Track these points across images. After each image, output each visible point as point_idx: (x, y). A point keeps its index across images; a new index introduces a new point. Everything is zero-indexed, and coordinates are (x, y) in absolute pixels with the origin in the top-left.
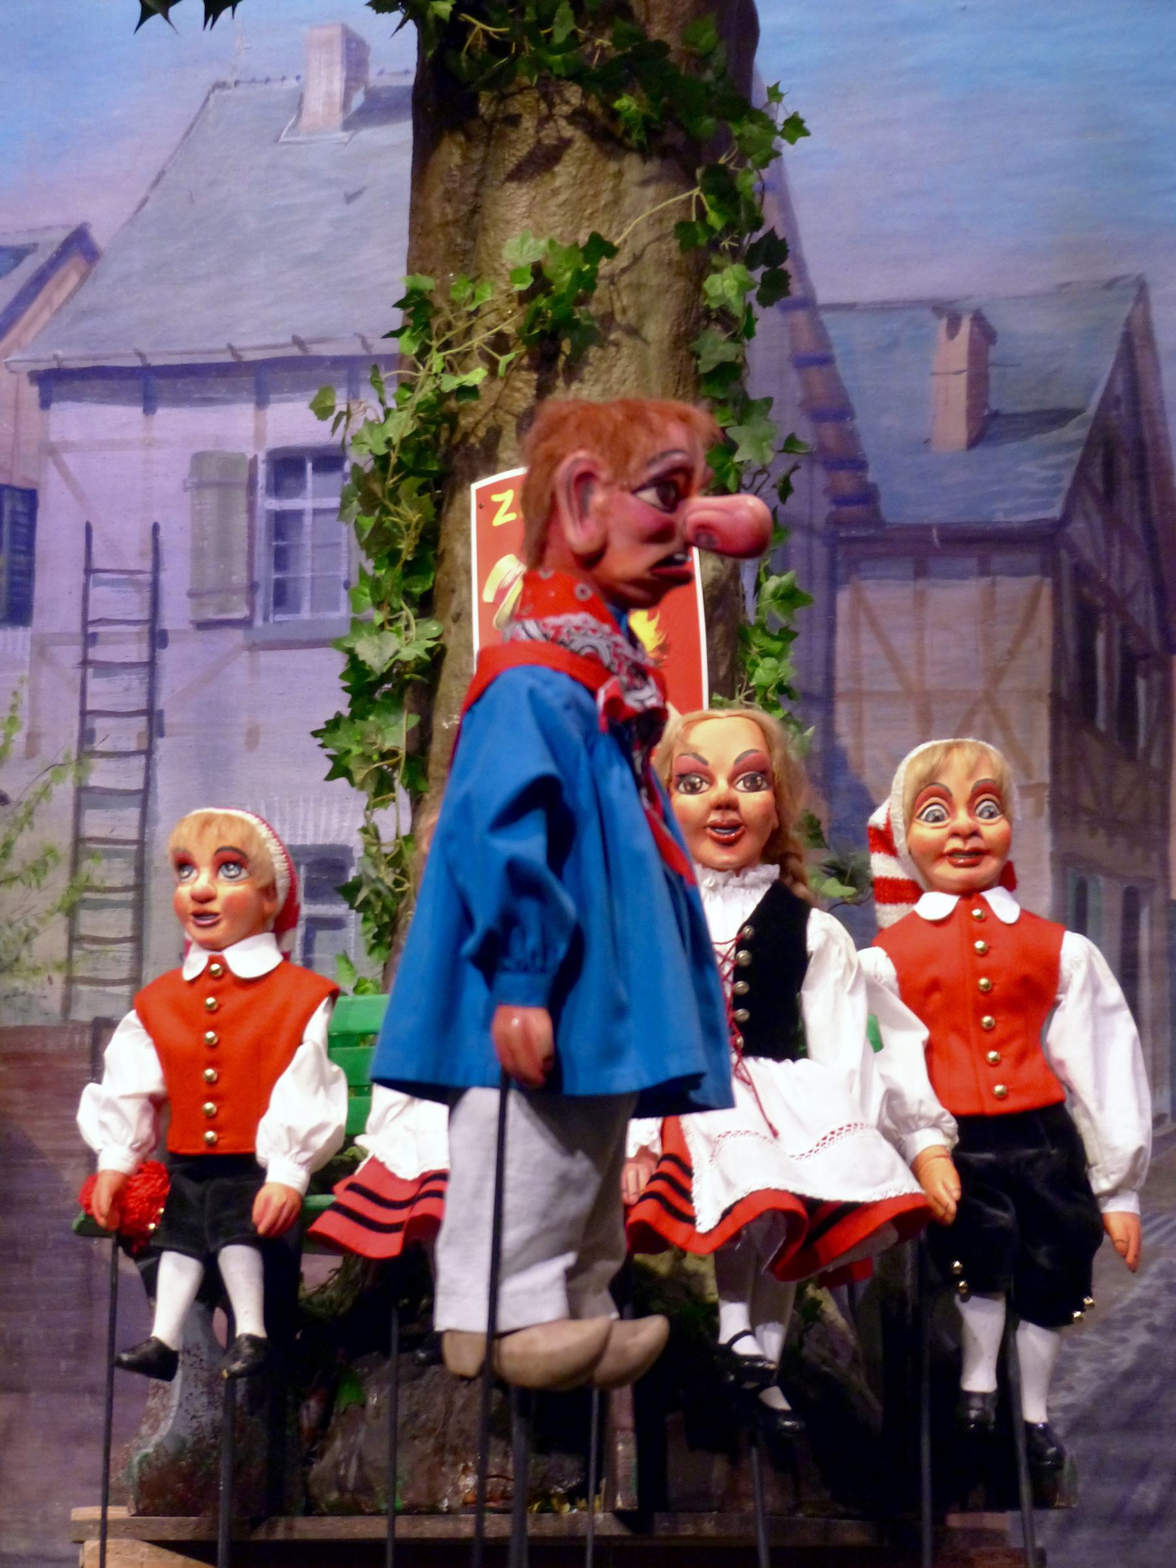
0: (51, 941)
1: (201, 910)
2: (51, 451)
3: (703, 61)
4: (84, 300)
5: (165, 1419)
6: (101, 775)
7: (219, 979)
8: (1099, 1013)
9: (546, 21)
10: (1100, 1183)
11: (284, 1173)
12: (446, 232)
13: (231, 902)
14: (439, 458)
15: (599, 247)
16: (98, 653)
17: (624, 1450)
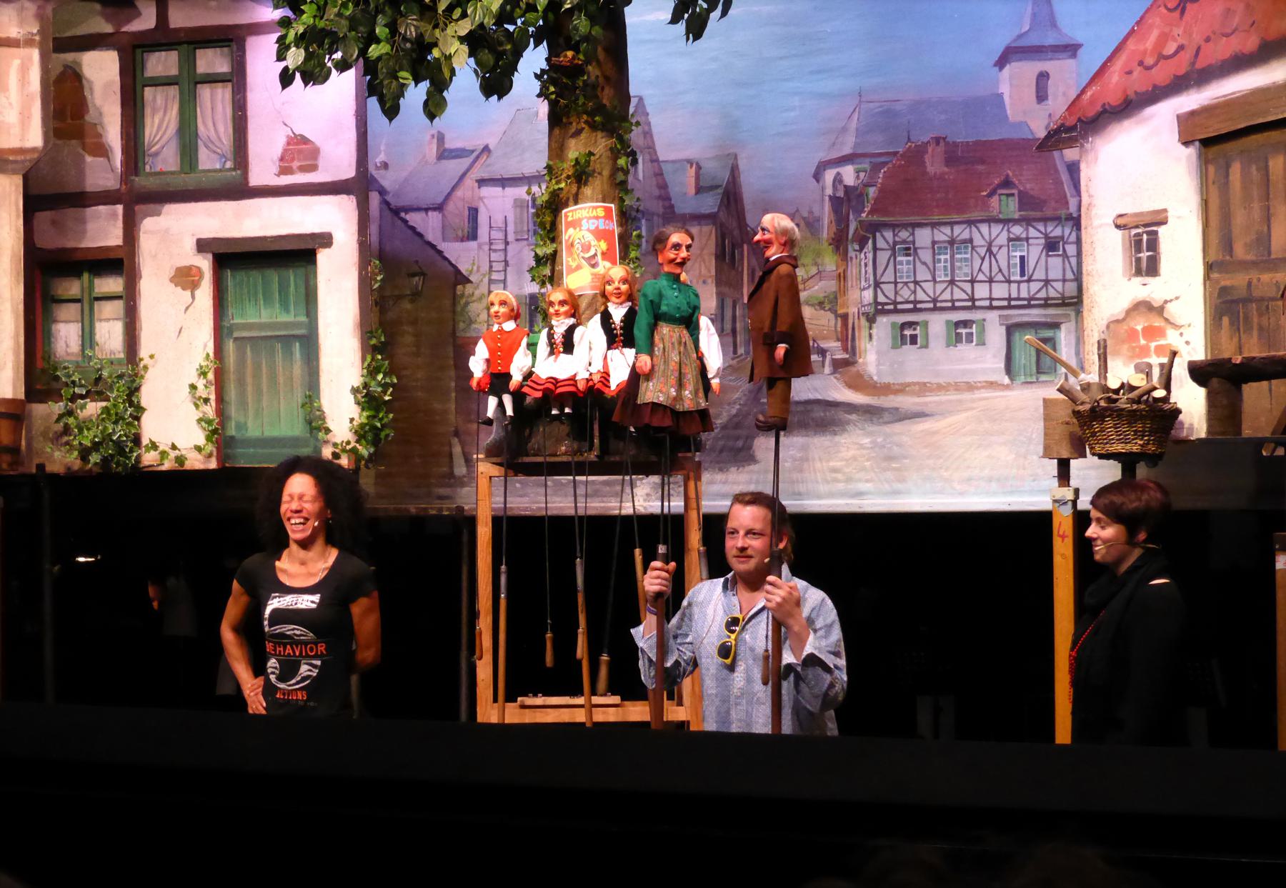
0: (484, 316)
1: (497, 315)
2: (481, 199)
3: (615, 108)
4: (488, 162)
5: (492, 435)
6: (495, 276)
7: (501, 331)
8: (709, 335)
9: (577, 99)
10: (710, 376)
11: (517, 377)
12: (557, 150)
13: (504, 314)
14: (555, 205)
15: (591, 154)
16: (493, 247)
17: (596, 441)
